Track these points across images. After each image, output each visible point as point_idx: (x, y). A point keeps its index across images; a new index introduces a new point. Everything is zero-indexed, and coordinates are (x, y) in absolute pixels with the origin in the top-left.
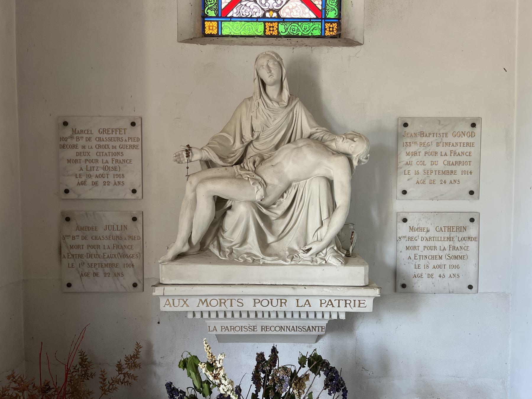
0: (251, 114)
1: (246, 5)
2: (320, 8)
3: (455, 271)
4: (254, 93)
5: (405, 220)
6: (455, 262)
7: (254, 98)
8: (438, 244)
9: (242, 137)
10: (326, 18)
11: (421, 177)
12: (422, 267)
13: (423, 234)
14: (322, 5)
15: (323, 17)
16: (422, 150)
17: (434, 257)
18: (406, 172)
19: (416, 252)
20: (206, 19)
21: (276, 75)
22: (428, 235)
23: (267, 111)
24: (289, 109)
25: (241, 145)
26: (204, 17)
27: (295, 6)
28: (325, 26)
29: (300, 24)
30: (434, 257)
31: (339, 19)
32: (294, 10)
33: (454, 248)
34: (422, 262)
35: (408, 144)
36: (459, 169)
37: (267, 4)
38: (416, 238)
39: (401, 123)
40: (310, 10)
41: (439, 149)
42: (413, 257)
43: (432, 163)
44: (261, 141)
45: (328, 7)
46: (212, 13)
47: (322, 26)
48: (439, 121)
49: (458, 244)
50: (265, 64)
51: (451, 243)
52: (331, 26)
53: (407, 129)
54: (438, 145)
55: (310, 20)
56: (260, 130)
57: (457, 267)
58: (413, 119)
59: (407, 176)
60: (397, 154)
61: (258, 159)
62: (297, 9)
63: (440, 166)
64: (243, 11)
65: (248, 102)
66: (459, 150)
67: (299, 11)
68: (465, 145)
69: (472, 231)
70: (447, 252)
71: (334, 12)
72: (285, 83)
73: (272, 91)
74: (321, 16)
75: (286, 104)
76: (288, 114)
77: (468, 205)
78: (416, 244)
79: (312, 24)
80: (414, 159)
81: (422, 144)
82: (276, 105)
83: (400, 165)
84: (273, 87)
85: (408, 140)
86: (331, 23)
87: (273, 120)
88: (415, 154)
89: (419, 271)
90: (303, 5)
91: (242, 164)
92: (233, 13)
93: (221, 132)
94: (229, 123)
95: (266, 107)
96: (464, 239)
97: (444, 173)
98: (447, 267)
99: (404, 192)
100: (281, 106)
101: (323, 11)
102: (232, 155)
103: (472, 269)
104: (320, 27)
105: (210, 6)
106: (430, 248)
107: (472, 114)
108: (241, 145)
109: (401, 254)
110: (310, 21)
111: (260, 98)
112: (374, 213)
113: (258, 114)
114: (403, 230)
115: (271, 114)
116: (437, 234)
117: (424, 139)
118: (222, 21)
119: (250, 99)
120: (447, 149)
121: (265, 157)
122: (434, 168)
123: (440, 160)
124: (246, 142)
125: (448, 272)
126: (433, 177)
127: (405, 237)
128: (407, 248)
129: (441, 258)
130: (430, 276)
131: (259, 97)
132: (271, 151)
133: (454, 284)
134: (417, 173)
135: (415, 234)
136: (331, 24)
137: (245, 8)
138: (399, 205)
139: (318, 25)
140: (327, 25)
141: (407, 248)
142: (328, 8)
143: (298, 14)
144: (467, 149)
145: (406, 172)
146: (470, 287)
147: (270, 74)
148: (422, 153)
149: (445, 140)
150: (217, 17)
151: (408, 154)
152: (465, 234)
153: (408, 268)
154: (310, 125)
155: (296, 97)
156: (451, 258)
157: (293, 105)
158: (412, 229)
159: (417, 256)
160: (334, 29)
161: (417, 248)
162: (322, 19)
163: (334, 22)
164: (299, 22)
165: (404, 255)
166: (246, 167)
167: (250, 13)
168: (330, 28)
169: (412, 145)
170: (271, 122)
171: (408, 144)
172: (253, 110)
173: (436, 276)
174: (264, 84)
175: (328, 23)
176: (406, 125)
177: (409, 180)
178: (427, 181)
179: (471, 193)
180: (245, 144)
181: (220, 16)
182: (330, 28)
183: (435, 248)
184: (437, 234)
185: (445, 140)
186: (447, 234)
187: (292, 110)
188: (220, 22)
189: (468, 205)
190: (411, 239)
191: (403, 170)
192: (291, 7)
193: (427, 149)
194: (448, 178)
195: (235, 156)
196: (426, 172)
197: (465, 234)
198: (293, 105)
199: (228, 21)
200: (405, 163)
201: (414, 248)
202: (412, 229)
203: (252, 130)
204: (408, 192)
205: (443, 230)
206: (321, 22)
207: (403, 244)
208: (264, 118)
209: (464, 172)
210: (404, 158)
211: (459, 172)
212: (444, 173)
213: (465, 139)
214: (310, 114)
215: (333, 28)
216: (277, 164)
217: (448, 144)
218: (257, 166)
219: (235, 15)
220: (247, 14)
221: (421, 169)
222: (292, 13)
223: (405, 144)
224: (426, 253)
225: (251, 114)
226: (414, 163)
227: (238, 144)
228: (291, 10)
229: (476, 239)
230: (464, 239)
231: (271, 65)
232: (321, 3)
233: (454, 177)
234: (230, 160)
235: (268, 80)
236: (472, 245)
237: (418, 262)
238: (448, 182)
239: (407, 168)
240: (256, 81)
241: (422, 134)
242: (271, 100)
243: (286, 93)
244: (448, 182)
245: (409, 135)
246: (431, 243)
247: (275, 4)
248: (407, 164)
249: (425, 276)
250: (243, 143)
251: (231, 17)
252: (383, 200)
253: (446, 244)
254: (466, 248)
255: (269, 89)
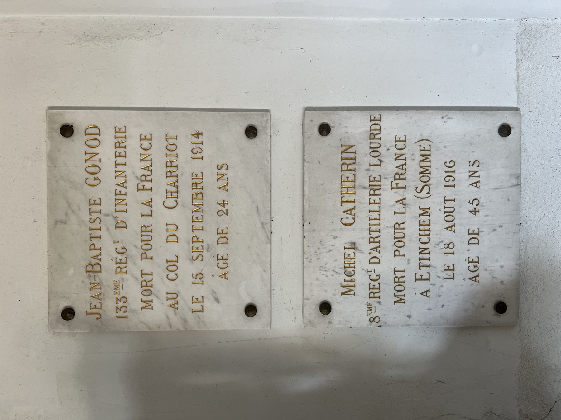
3: (462, 173)
5: (325, 307)
6: (437, 174)
8: (388, 219)
11: (208, 266)
12: (449, 260)
13: (362, 260)
16: (137, 266)
17: (425, 229)
18: (197, 306)
19: (409, 278)
22: (365, 246)
30: (425, 229)
33: (399, 176)
34: (438, 259)
35: (120, 304)
36: (187, 167)
38: (373, 277)
39: (63, 327)
41: (134, 221)
42: (424, 286)
43: (172, 236)
48: (57, 223)
49: (390, 166)
51: (386, 184)
53: (80, 309)
54: (121, 225)
57: (450, 166)
58: (52, 294)
59: (207, 304)
60: (150, 338)
63: (181, 217)
66: (134, 166)
68: (121, 150)
69: (355, 128)
70: (410, 195)
77: (286, 138)
78: (387, 277)
80: (161, 286)
81: (121, 267)
83: (176, 321)
85: (110, 305)
88: (147, 288)
89: (462, 268)
96: (375, 151)
97: (198, 207)
98: (449, 193)
99: (251, 310)
103: (457, 126)
106: (399, 241)
107: (39, 134)
109: (414, 315)
112: (306, 384)
114: (351, 312)
116: (363, 221)
117: (108, 263)
120: (134, 200)
122: (184, 233)
123: (163, 217)
125: (464, 191)
126: (209, 237)
127: (370, 307)
128: (400, 300)
129: (425, 212)
130: (474, 237)
133: (494, 173)
134: (199, 277)
135: (362, 280)
138: (287, 321)
141: (400, 300)
144: (133, 144)
145: (197, 306)
146: (505, 130)
148: (146, 266)
149: (108, 206)
151: (148, 305)
152: (363, 149)
153: (453, 296)
156: (426, 184)
158: (348, 290)
159: (420, 273)
161: (399, 275)
165: (417, 307)
169: (123, 293)
171: (120, 304)
173: (475, 223)
176: (68, 314)
177: (217, 300)
178: (221, 250)
179: (251, 132)
183: (398, 226)
184: (363, 221)
185: (108, 206)
186: (363, 195)
189: (286, 138)
190: (374, 292)
191: (190, 317)
193: (135, 253)
194: (213, 195)
196: (197, 252)
197: (363, 149)
200: (171, 311)
201: (399, 281)
202: (348, 290)
204: (248, 301)
205: (351, 206)
207: (387, 308)
209: (197, 153)
210: (158, 314)
211: (197, 166)
212: (198, 207)
213: (106, 152)
217: (120, 196)
221: (187, 269)
223: (120, 313)
224: (412, 249)
226: (171, 287)
229: (375, 113)
230: (375, 151)
233: (210, 181)
236: (391, 127)
237: (437, 272)
238: (222, 196)
239: (185, 304)
241: (93, 267)
244: (222, 196)
245: (96, 302)
246: (387, 237)
248: (175, 306)
249: (474, 252)
252: (271, 362)
253: (389, 197)
254: (400, 145)
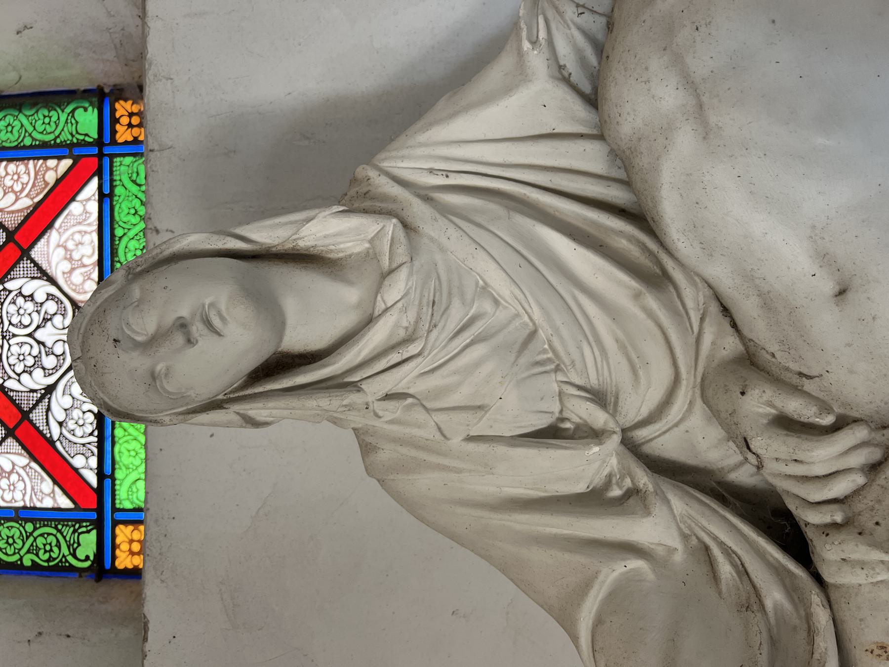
0: (456, 441)
1: (61, 424)
2: (66, 163)
4: (335, 421)
7: (358, 420)
9: (593, 500)
10: (99, 142)
14: (60, 158)
15: (96, 151)
20: (108, 565)
21: (215, 293)
23: (437, 344)
24: (418, 210)
25: (658, 509)
26: (102, 569)
27: (61, 251)
28: (126, 143)
29: (119, 232)
31: (102, 97)
32: (76, 256)
37: (58, 349)
40: (73, 199)
44: (618, 373)
45: (63, 138)
46: (88, 543)
47: (124, 155)
50: (138, 362)
52: (125, 120)
55: (105, 197)
56: (551, 384)
61: (759, 403)
62: (70, 245)
64: (79, 432)
65: (386, 454)
67: (77, 237)
71: (79, 113)
72: (267, 234)
73: (312, 314)
74: (94, 159)
75: (391, 226)
76: (446, 211)
79: (118, 190)
82: (394, 291)
84: (291, 306)
86: (115, 121)
87: (488, 306)
90: (57, 224)
91: (812, 517)
92: (87, 467)
93: (575, 639)
94: (511, 570)
95: (413, 349)
100: (402, 253)
101: (77, 152)
102: (725, 569)
104: (128, 160)
105: (65, 550)
108: (658, 509)
110: (111, 195)
111: (355, 387)
113: (455, 399)
115: (456, 315)
118: (114, 509)
119: (367, 449)
121: (731, 345)
124: (626, 472)
131: (353, 398)
132: (680, 314)
136: (117, 121)
137: (71, 425)
139: (124, 167)
140: (123, 134)
142: (66, 137)
143: (87, 238)
147: (197, 329)
150: (98, 524)
154: (508, 90)
155: (354, 181)
157: (395, 190)
160: (135, 109)
162: (101, 155)
163: (113, 111)
164: (113, 236)
166: (840, 488)
167: (86, 407)
168: (130, 125)
170: (501, 315)
172: (429, 433)
174: (279, 365)
175: (114, 132)
180: (643, 479)
181: (94, 516)
182: (130, 125)
187: (425, 195)
188: (119, 516)
192: (66, 266)
195: (728, 552)
198: (395, 190)
199: (113, 485)
203: (551, 434)
206: (112, 156)
208: (477, 364)
214: (442, 103)
215: (131, 115)
216: (824, 258)
218: (825, 407)
219: (94, 462)
220: (90, 418)
222: (86, 261)
225: (456, 441)
227: (654, 529)
228: (76, 265)
231: (146, 324)
232: (52, 163)
234: (774, 596)
235: (240, 342)
240: (257, 410)
242: (369, 321)
243: (327, 229)
247: (58, 320)
250: (633, 493)
251: (101, 474)
255: (299, 336)
